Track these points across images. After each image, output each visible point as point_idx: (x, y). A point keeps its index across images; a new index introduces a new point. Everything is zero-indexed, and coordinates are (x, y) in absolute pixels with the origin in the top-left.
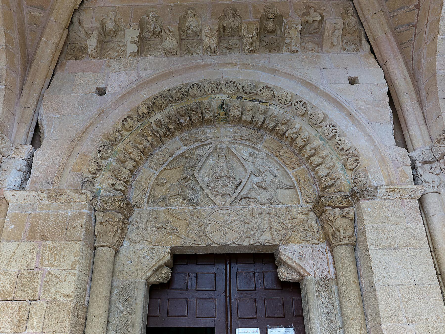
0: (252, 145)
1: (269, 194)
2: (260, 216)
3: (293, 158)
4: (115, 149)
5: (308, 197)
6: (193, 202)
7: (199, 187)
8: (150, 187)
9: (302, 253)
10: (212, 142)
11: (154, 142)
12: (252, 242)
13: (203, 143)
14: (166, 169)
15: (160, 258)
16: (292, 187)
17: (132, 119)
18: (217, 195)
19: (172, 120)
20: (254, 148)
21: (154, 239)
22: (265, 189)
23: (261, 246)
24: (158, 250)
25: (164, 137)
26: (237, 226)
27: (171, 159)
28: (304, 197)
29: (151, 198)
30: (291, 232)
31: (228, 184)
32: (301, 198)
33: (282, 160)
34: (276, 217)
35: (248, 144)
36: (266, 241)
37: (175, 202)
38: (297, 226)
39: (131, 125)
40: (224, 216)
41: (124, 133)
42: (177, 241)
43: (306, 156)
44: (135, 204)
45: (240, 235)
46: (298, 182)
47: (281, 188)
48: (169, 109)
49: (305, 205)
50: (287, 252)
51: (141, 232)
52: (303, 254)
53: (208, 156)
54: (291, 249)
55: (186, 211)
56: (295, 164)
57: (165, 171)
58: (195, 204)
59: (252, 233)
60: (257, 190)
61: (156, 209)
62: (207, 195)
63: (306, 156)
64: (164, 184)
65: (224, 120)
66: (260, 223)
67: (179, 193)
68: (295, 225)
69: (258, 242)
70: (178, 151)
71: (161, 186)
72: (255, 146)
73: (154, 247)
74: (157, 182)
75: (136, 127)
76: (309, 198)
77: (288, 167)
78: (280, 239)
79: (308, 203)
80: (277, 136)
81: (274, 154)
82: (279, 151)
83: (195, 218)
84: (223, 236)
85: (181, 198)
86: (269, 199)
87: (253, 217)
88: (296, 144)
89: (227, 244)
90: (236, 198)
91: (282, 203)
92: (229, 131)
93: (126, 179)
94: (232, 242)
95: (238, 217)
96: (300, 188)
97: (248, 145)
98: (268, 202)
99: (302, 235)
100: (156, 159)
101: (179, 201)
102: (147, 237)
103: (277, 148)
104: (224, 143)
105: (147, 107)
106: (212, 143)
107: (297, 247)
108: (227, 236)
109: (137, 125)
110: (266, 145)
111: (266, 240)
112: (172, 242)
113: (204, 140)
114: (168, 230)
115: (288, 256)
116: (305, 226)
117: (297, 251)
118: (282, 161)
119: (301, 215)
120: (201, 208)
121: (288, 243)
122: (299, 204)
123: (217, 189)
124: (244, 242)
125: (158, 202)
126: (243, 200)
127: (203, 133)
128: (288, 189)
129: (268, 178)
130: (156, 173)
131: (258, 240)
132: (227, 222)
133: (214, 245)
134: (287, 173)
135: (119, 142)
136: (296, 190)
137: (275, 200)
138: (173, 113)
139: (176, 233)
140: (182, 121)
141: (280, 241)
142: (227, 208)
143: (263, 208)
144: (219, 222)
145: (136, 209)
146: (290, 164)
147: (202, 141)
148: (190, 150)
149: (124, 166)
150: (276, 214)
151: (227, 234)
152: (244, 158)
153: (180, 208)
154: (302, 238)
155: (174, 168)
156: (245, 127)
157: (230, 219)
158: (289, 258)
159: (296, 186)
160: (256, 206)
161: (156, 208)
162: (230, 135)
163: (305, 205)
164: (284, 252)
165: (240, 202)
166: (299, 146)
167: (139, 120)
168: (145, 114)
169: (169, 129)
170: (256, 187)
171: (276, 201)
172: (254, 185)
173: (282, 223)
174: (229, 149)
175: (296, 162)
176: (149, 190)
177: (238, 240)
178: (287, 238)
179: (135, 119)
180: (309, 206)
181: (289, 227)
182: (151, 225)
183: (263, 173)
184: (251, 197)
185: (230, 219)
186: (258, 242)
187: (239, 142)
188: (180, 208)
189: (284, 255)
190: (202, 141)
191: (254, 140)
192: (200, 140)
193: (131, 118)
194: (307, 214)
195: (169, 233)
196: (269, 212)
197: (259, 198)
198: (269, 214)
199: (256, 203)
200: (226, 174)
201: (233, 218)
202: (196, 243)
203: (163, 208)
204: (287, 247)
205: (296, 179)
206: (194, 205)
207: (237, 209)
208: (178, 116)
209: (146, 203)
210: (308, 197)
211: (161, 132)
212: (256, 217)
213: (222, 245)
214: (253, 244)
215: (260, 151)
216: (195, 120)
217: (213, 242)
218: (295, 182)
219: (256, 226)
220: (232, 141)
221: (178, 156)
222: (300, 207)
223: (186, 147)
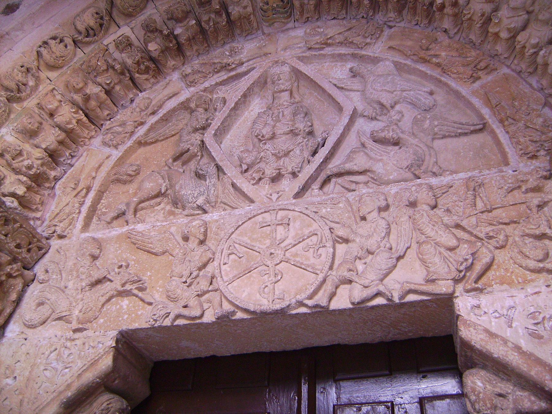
0: (356, 52)
1: (408, 154)
2: (384, 214)
3: (469, 55)
4: (20, 109)
5: (532, 141)
6: (195, 205)
7: (212, 170)
8: (96, 186)
9: (542, 316)
10: (255, 65)
11: (112, 85)
12: (358, 294)
13: (233, 73)
14: (143, 142)
15: (85, 365)
16: (478, 127)
17: (62, 41)
18: (260, 179)
19: (152, 32)
20: (362, 58)
21: (77, 312)
22: (396, 143)
23: (391, 306)
24: (84, 344)
25: (138, 73)
26: (311, 250)
27: (154, 119)
28: (518, 143)
29: (98, 213)
30: (492, 248)
31: (291, 148)
32: (509, 148)
33: (438, 65)
34: (435, 210)
35: (343, 52)
36: (407, 287)
37: (153, 215)
38: (509, 229)
39: (58, 54)
40: (274, 227)
41: (44, 74)
42: (137, 315)
43: (504, 35)
44: (53, 229)
45: (321, 277)
46: (494, 108)
47: (444, 137)
48: (149, 13)
49: (526, 165)
50: (484, 318)
51: (49, 296)
52: (544, 318)
53: (245, 96)
54: (497, 306)
55: (173, 229)
56: (479, 67)
57: (142, 151)
58: (200, 212)
59: (360, 267)
60: (372, 150)
61: (100, 236)
62: (233, 185)
63: (504, 35)
64: (130, 175)
65: (278, 12)
66: (383, 235)
67: (163, 191)
68: (501, 226)
69: (378, 294)
70: (173, 99)
71: (125, 182)
72: (363, 53)
73: (77, 335)
74: (115, 174)
75: (72, 59)
76: (536, 142)
77: (459, 78)
78: (454, 274)
79: (534, 157)
80: (417, 18)
81: (415, 58)
82: (428, 49)
83: (193, 244)
84: (268, 284)
85: (168, 203)
86: (409, 167)
87: (363, 222)
88: (469, 16)
89: (278, 307)
90: (312, 179)
91: (453, 172)
92: (295, 37)
93: (34, 170)
94: (294, 301)
95: (315, 226)
96: (501, 121)
97: (345, 55)
98: (409, 175)
99: (532, 254)
100: (118, 124)
101: (162, 212)
102: (62, 307)
103: (421, 42)
104: (284, 63)
105: (97, 13)
106: (254, 68)
107: (520, 296)
108: (280, 283)
109: (75, 55)
110: (392, 43)
111: (407, 282)
112: (126, 316)
113: (234, 66)
114: (117, 285)
115: (487, 331)
116: (535, 225)
117: (519, 309)
118: (439, 70)
119: (518, 196)
120: (213, 216)
121: (485, 285)
122: (507, 164)
123: (262, 165)
124: (335, 299)
125: (108, 219)
126: (333, 180)
127: (233, 52)
128: (466, 134)
129: (406, 118)
130: (116, 154)
131: (377, 285)
132: (283, 245)
133: (240, 315)
134: (457, 94)
135: (29, 92)
136: (493, 133)
137: (430, 169)
138: (158, 19)
139: (136, 292)
140: (178, 31)
141: (457, 281)
142: (280, 207)
143: (393, 192)
144: (257, 245)
145: (55, 243)
146: (462, 69)
147: (230, 68)
148: (201, 93)
149: (35, 142)
150: (433, 203)
151: (279, 277)
152: (335, 85)
153: (159, 224)
154: (532, 264)
155: (162, 138)
156: (334, 18)
157: (292, 233)
158: (492, 335)
159: (490, 121)
160: (371, 191)
161: (99, 235)
162: (297, 44)
163: (526, 165)
164: (473, 318)
165: (326, 189)
166: (476, 18)
167: (80, 45)
168: (92, 29)
169: (148, 52)
170: (370, 143)
171: (434, 170)
172: (364, 139)
173: (458, 226)
174: (297, 74)
175: (480, 62)
176: (92, 195)
177: (315, 293)
178: (478, 268)
179: (69, 41)
180: (542, 165)
181: (482, 235)
182: (78, 276)
183: (389, 108)
184: (356, 168)
185: (292, 233)
186: (378, 294)
187: (322, 52)
188: (159, 224)
189: (475, 325)
190: (230, 68)
191: (358, 40)
192: (225, 67)
193: (58, 40)
194: (537, 189)
195: (122, 294)
196: (411, 200)
197: (379, 168)
198: (413, 204)
199: (370, 184)
200: (286, 129)
201: (300, 232)
202: (186, 312)
203: (117, 231)
204: (484, 300)
205: (488, 102)
206: (198, 214)
207: (313, 203)
208: (170, 24)
209: (79, 224)
210: (532, 141)
211: (129, 62)
212: (369, 217)
213: (264, 314)
214: (363, 301)
215: (375, 60)
216: (208, 24)
217: (237, 307)
218: (486, 112)
219: (371, 244)
220: (304, 55)
221: (173, 111)
222: (510, 172)
223: (192, 89)
